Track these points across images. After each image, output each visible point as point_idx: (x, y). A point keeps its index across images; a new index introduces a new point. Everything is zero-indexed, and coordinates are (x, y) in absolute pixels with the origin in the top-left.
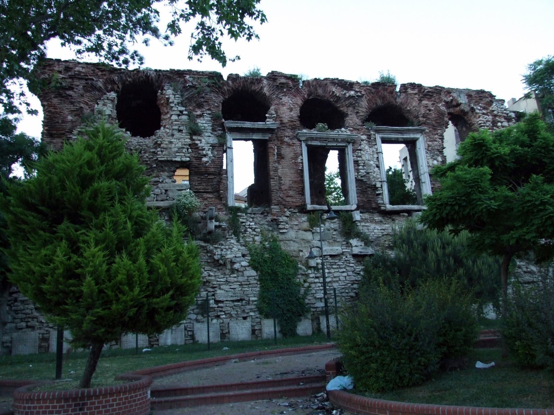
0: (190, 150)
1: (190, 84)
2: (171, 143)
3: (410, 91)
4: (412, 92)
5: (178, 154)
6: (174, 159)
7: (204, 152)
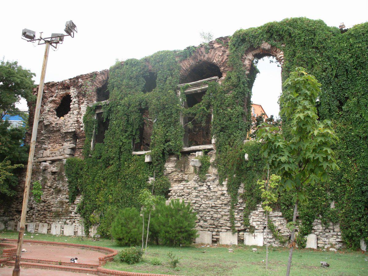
0: (76, 125)
1: (81, 84)
2: (69, 121)
3: (216, 46)
4: (218, 46)
5: (70, 128)
6: (69, 131)
7: (81, 125)
